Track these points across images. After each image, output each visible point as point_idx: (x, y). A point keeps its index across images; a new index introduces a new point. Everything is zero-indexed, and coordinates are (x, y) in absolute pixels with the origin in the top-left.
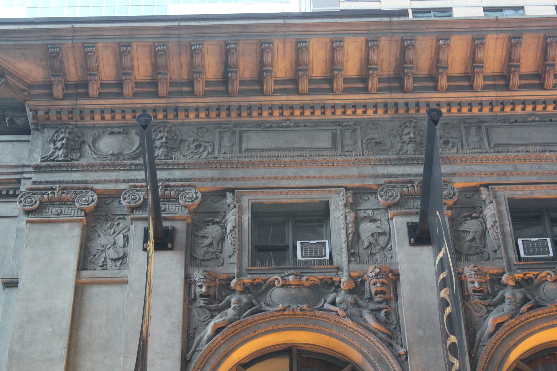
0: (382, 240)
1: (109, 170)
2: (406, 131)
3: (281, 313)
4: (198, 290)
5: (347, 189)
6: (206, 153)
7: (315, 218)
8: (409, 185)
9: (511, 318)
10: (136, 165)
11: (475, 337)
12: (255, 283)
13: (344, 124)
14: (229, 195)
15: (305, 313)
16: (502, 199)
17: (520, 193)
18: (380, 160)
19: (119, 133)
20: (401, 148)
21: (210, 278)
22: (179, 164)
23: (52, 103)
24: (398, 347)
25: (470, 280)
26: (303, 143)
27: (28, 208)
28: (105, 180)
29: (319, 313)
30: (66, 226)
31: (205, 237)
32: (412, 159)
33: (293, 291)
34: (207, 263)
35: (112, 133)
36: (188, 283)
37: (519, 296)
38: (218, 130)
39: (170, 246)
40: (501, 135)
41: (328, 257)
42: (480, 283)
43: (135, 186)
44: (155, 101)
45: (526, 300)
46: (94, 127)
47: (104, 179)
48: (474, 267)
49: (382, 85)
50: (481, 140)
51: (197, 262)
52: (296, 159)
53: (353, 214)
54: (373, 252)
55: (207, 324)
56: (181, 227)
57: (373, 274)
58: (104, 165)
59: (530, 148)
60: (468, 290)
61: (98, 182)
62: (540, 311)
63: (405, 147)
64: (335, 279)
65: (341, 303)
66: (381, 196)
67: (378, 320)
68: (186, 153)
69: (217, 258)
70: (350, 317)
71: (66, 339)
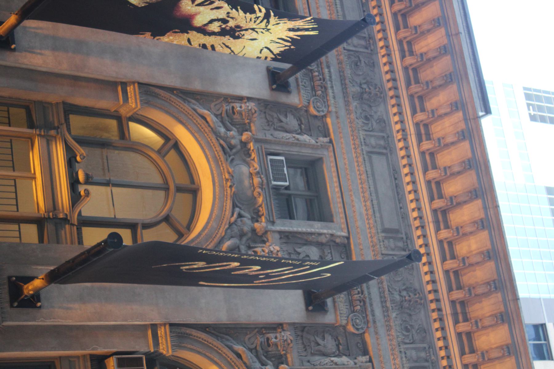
3: (226, 170)
8: (321, 77)
11: (226, 335)
12: (251, 151)
13: (371, 41)
15: (229, 189)
18: (384, 292)
25: (278, 335)
31: (323, 338)
34: (300, 342)
39: (311, 308)
48: (291, 340)
52: (397, 349)
60: (269, 333)
63: (395, 293)
69: (268, 125)
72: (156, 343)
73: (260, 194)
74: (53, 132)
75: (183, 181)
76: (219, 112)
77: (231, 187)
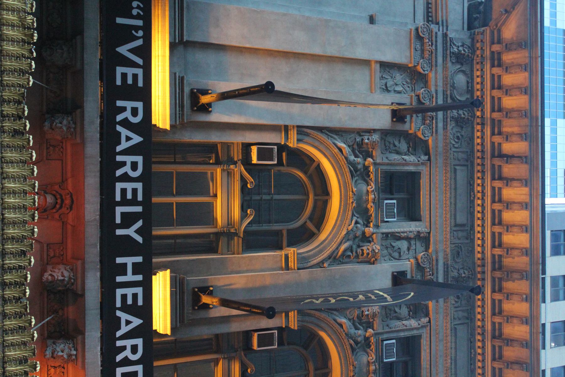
0: (396, 255)
1: (444, 81)
2: (466, 272)
3: (351, 190)
4: (366, 137)
5: (429, 233)
6: (454, 143)
7: (411, 212)
9: (345, 334)
10: (447, 98)
14: (427, 157)
15: (351, 205)
16: (421, 331)
17: (424, 343)
19: (468, 87)
20: (454, 268)
21: (374, 145)
22: (447, 126)
23: (488, 44)
24: (328, 262)
25: (370, 309)
26: (459, 205)
27: (420, 30)
28: (436, 79)
29: (350, 213)
30: (408, 54)
32: (447, 275)
33: (364, 197)
35: (468, 82)
36: (370, 131)
37: (359, 339)
38: (469, 151)
40: (462, 332)
41: (386, 220)
42: (368, 315)
43: (433, 97)
44: (489, 110)
45: (357, 343)
46: (472, 71)
47: (438, 77)
49: (497, 257)
50: (460, 319)
51: (384, 137)
53: (412, 237)
54: (389, 249)
55: (345, 143)
56: (406, 127)
57: (374, 248)
58: (447, 78)
59: (453, 351)
61: (436, 73)
62: (350, 351)
64: (371, 225)
65: (357, 227)
66: (424, 255)
67: (345, 251)
68: (454, 130)
69: (386, 149)
70: (348, 233)
71: (337, 55)
72: (287, 138)
73: (372, 207)
76: (351, 317)
77: (352, 202)
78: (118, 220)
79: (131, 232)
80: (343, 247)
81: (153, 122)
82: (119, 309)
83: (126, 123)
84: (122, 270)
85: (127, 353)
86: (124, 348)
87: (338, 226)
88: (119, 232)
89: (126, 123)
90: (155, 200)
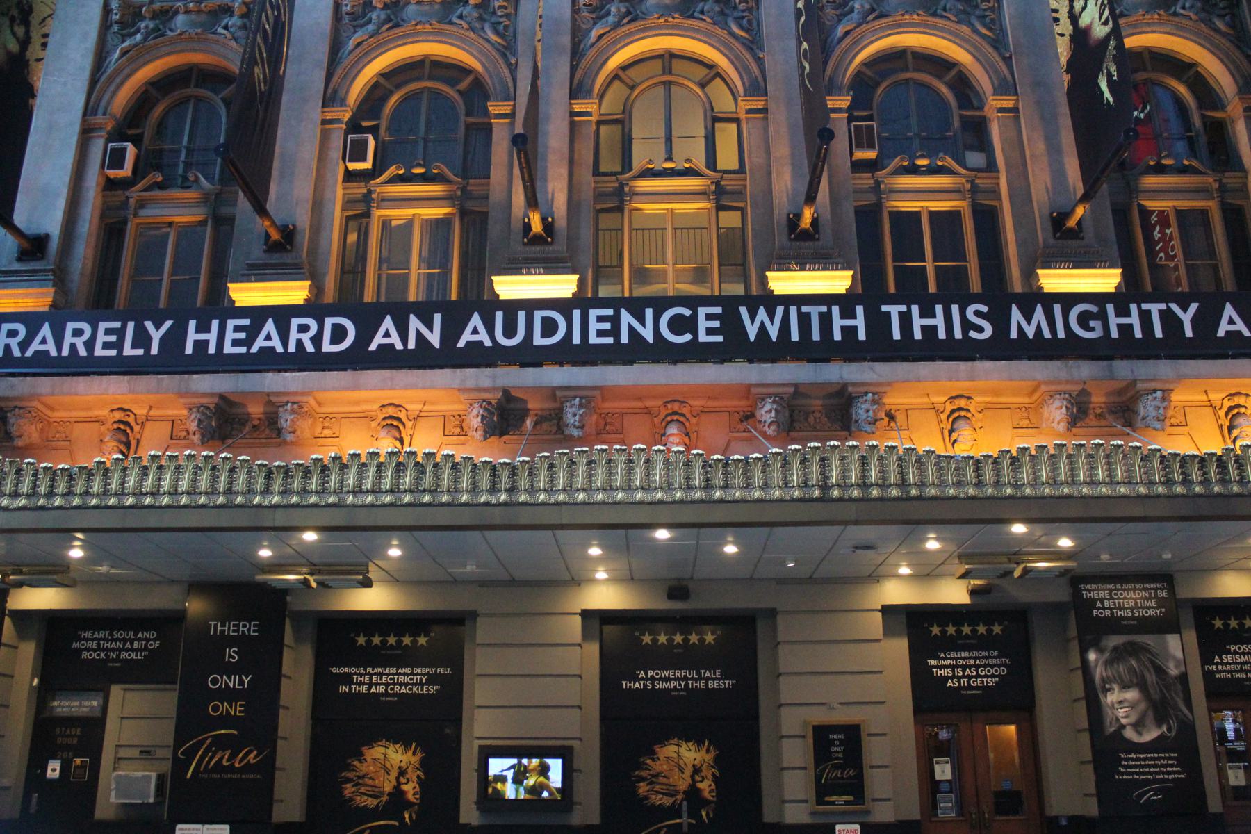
37: (383, 16)
45: (628, 13)
74: (626, 189)
75: (658, 65)
78: (140, 352)
79: (156, 335)
80: (493, 37)
81: (46, 309)
82: (249, 349)
83: (24, 346)
84: (201, 345)
85: (306, 338)
86: (300, 343)
87: (463, 43)
88: (154, 351)
89: (24, 346)
90: (162, 305)
